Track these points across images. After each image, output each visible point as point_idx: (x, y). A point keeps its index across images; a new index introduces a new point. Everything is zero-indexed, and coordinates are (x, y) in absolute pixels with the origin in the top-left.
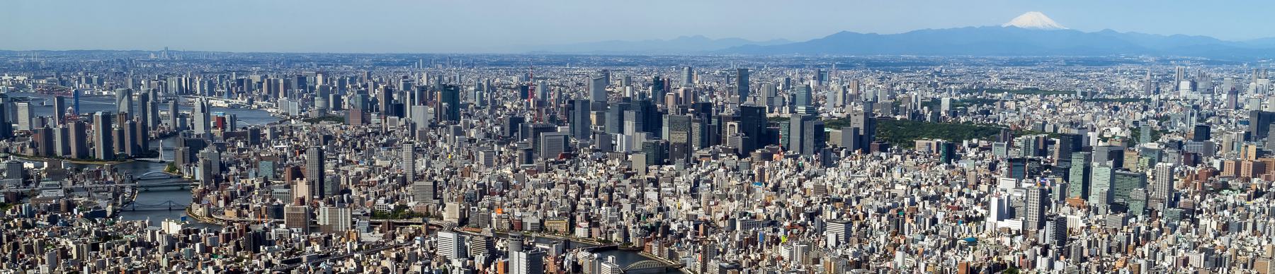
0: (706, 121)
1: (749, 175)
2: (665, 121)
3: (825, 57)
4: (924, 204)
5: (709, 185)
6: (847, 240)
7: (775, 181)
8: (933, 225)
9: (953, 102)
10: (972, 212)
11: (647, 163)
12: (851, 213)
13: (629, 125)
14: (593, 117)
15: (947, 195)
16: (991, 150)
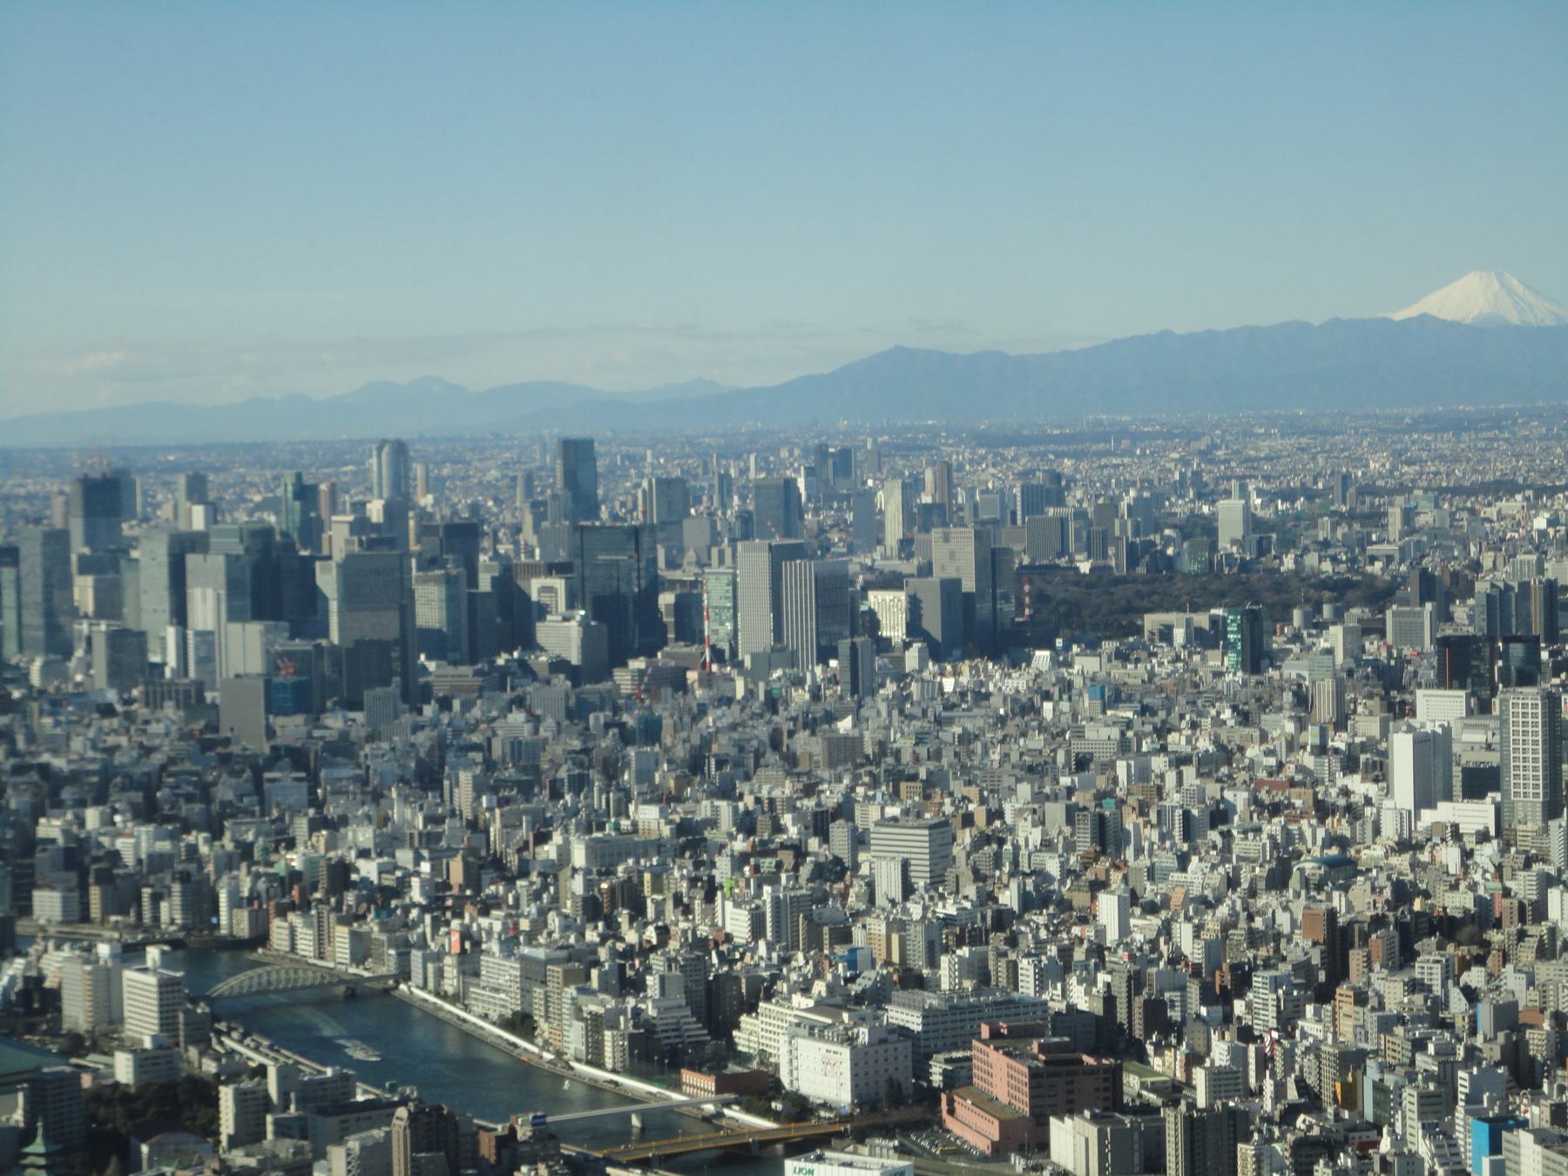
0: (463, 581)
1: (608, 726)
2: (327, 580)
3: (842, 429)
4: (1180, 776)
5: (478, 757)
6: (936, 880)
7: (696, 740)
8: (1213, 826)
9: (1253, 523)
10: (1334, 792)
11: (269, 709)
12: (948, 809)
13: (204, 599)
14: (84, 591)
15: (1253, 751)
16: (1382, 634)
